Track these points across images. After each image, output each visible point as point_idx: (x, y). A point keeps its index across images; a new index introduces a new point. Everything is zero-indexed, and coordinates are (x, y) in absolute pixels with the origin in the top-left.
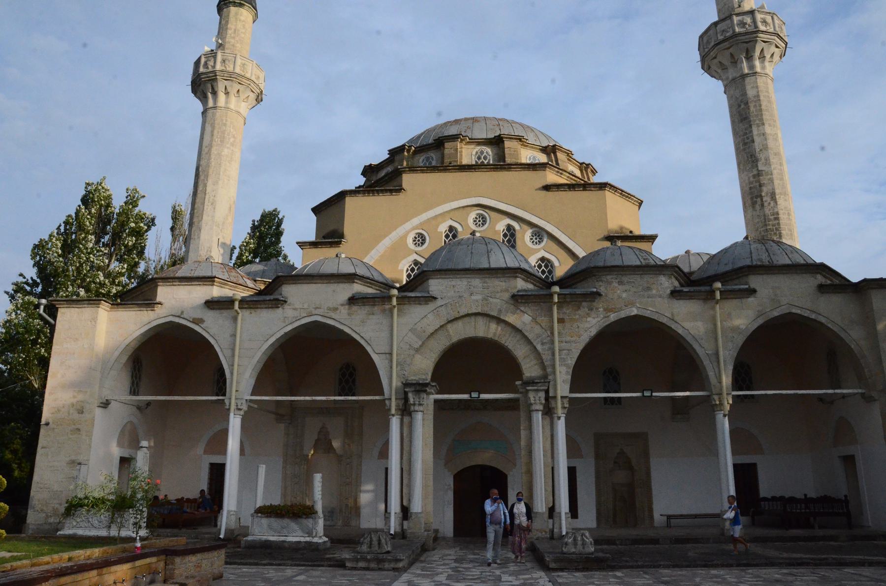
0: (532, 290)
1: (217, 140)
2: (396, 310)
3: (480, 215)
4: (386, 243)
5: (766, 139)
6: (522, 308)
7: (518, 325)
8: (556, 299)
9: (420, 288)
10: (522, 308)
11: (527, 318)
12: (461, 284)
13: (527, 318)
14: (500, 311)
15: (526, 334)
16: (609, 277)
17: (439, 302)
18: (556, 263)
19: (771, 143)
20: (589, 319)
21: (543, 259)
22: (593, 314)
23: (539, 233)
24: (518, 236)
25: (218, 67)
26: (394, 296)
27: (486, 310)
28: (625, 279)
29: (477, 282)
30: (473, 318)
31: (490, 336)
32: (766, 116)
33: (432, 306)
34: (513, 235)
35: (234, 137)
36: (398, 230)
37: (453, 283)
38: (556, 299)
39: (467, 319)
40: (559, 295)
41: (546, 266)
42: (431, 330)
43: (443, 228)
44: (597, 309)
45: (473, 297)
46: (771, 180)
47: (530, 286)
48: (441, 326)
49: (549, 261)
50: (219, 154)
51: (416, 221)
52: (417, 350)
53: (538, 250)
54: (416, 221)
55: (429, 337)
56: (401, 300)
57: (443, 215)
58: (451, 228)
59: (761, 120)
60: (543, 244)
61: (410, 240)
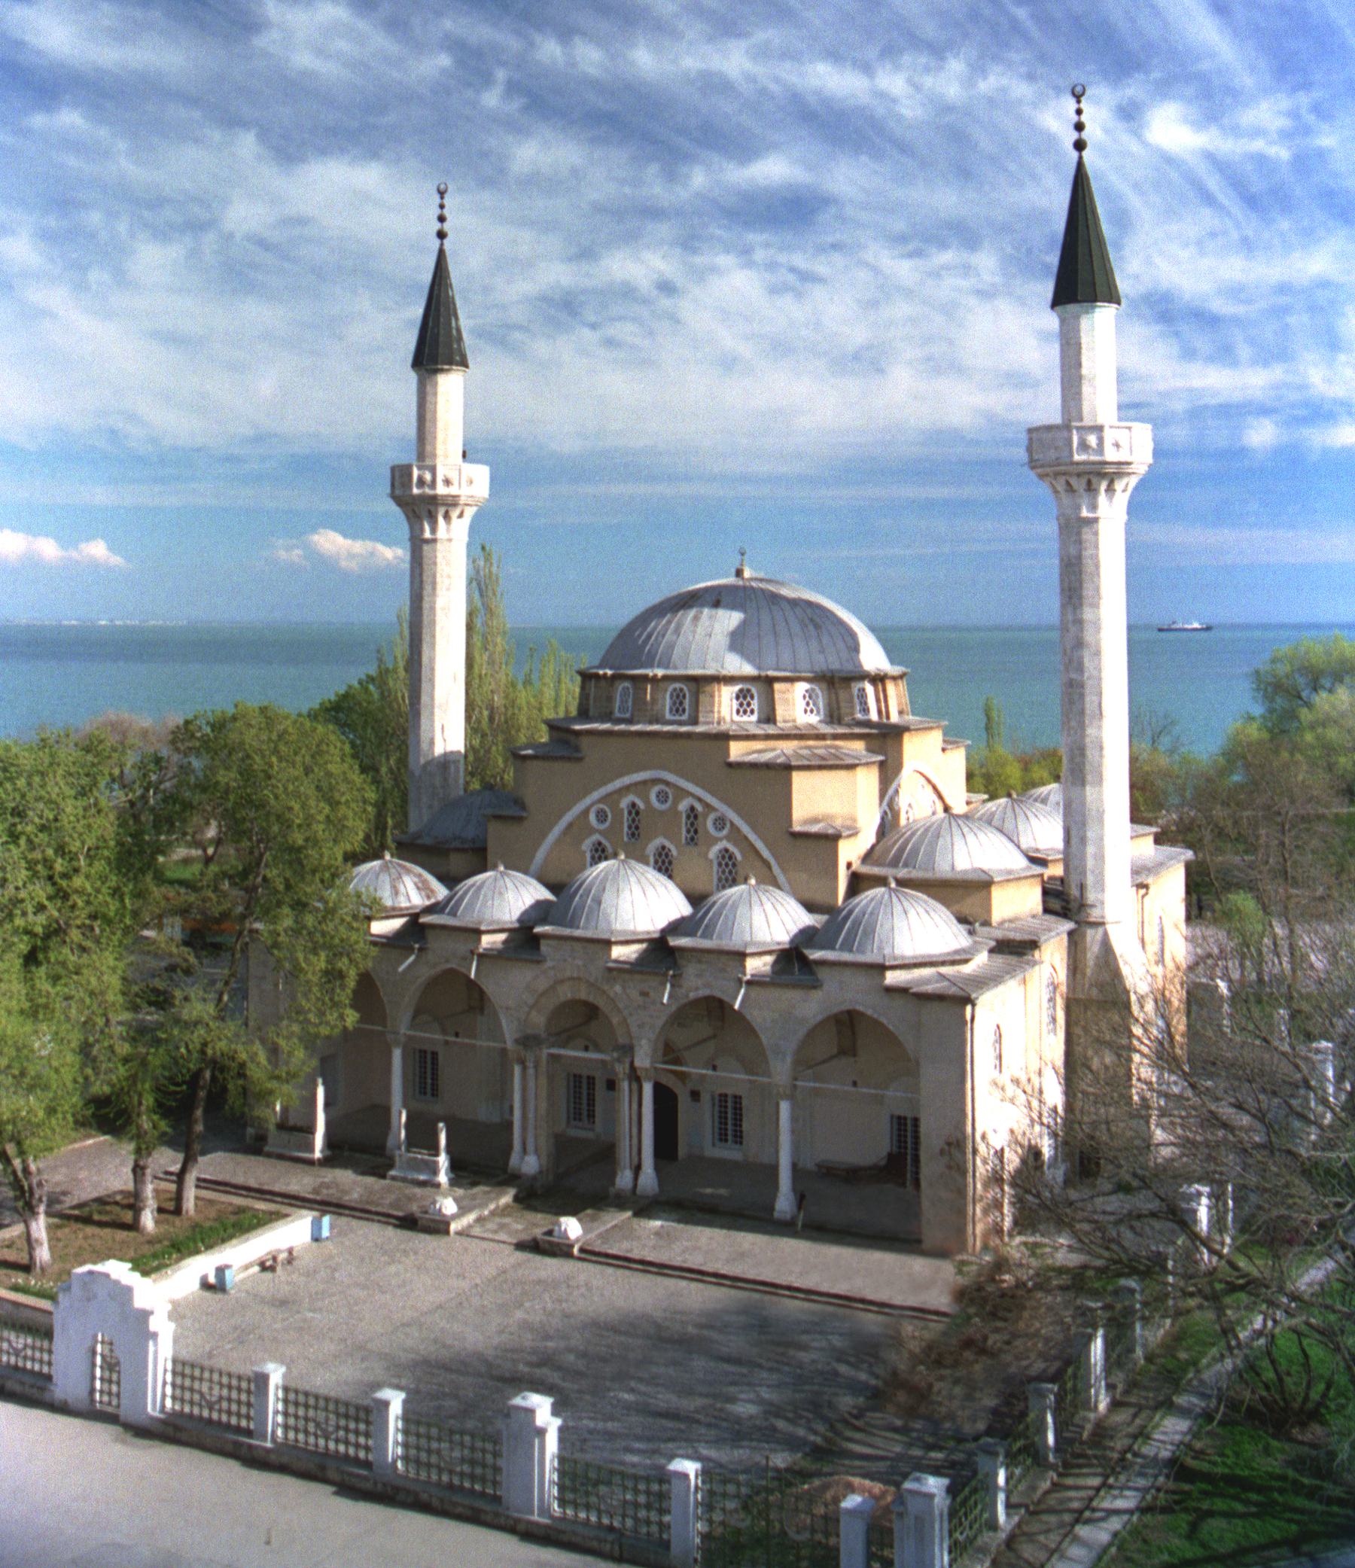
1: (428, 588)
4: (568, 817)
5: (1082, 630)
7: (612, 994)
11: (618, 988)
13: (618, 988)
19: (1088, 636)
24: (700, 818)
25: (415, 491)
32: (1088, 591)
34: (696, 817)
35: (449, 577)
41: (730, 858)
43: (624, 803)
46: (1082, 696)
50: (433, 609)
51: (596, 795)
52: (531, 1007)
53: (721, 839)
54: (596, 795)
58: (634, 805)
59: (1080, 597)
60: (725, 832)
61: (592, 818)
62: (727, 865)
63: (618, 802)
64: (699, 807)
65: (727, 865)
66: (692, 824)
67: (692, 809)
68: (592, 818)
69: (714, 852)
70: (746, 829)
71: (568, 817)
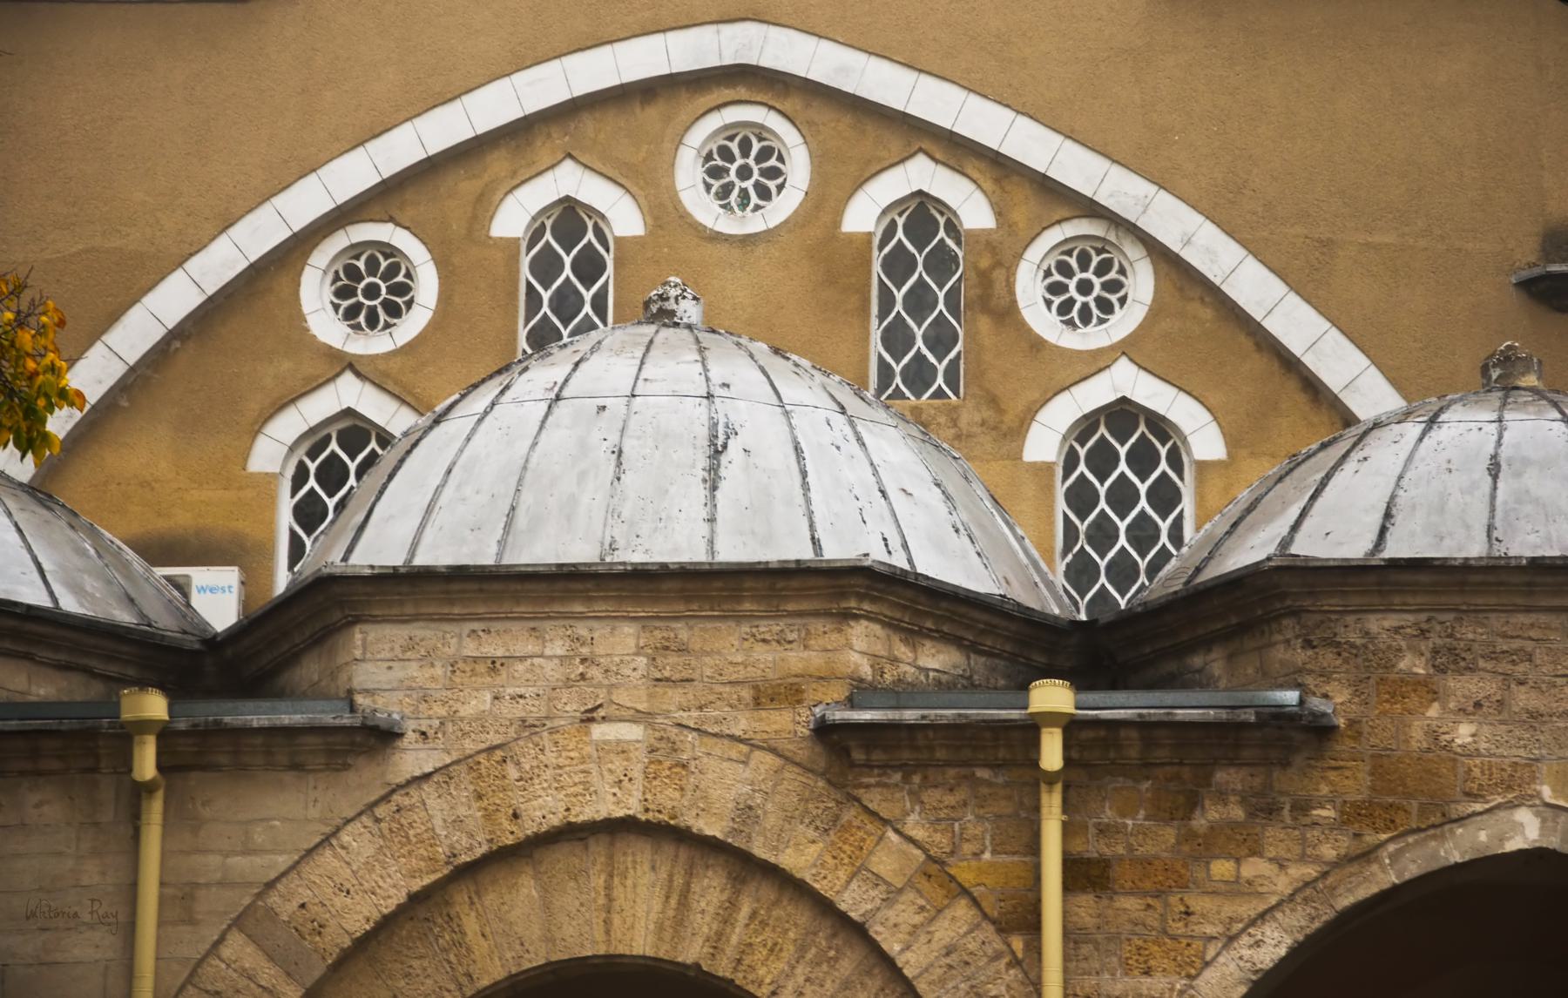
0: (945, 687)
2: (155, 810)
3: (745, 136)
6: (873, 799)
8: (1052, 754)
9: (309, 670)
10: (873, 799)
12: (539, 654)
14: (746, 813)
15: (892, 947)
16: (1378, 624)
17: (412, 759)
18: (1205, 439)
20: (1253, 868)
21: (1122, 414)
22: (1276, 838)
23: (1100, 251)
26: (144, 726)
27: (669, 802)
28: (1468, 632)
29: (620, 642)
30: (598, 847)
31: (691, 952)
33: (364, 781)
36: (239, 231)
37: (493, 648)
38: (1052, 754)
39: (562, 858)
40: (1072, 727)
41: (1143, 460)
42: (358, 916)
43: (513, 217)
44: (1302, 807)
45: (599, 731)
47: (937, 659)
48: (416, 899)
49: (1160, 426)
51: (353, 173)
53: (1097, 362)
55: (346, 959)
56: (186, 754)
57: (521, 135)
58: (569, 217)
60: (1125, 322)
61: (314, 292)
62: (1123, 497)
63: (484, 206)
64: (973, 209)
65: (1123, 497)
66: (920, 301)
67: (922, 212)
68: (314, 292)
69: (1045, 440)
70: (1253, 286)
71: (173, 299)
